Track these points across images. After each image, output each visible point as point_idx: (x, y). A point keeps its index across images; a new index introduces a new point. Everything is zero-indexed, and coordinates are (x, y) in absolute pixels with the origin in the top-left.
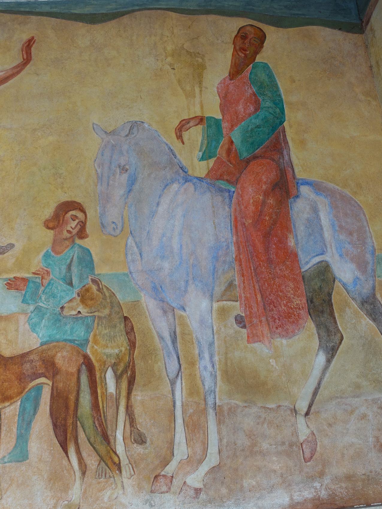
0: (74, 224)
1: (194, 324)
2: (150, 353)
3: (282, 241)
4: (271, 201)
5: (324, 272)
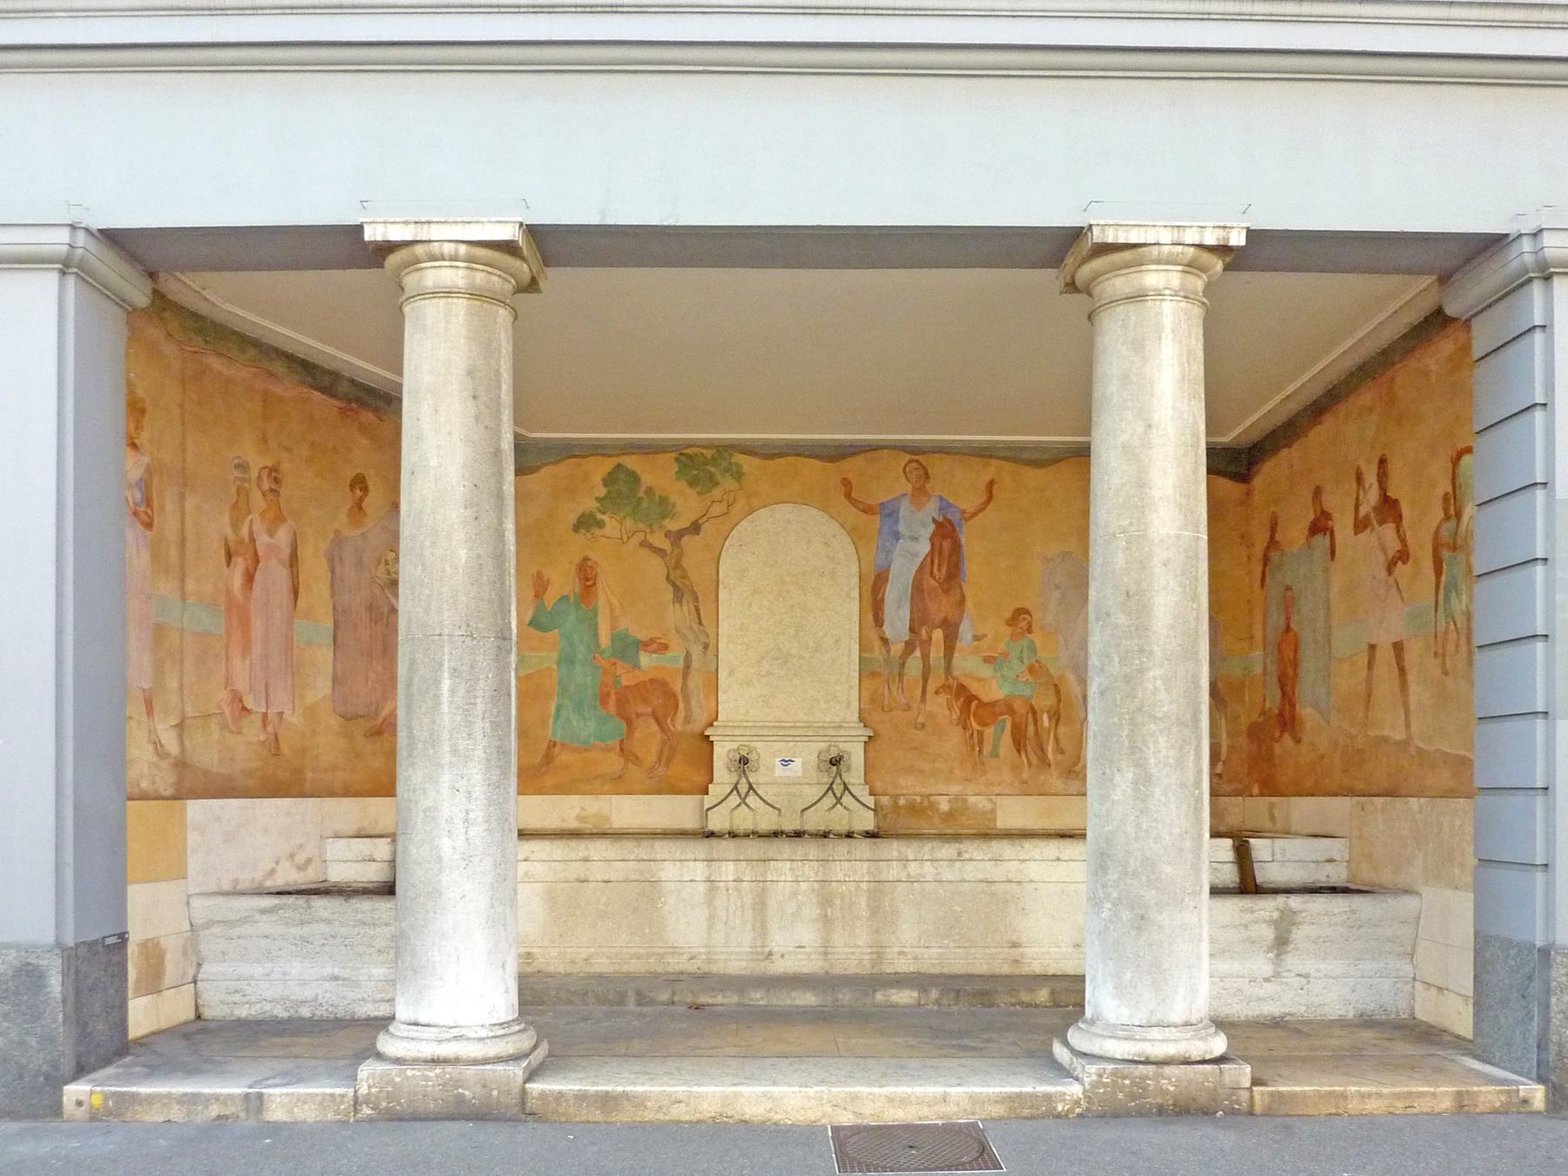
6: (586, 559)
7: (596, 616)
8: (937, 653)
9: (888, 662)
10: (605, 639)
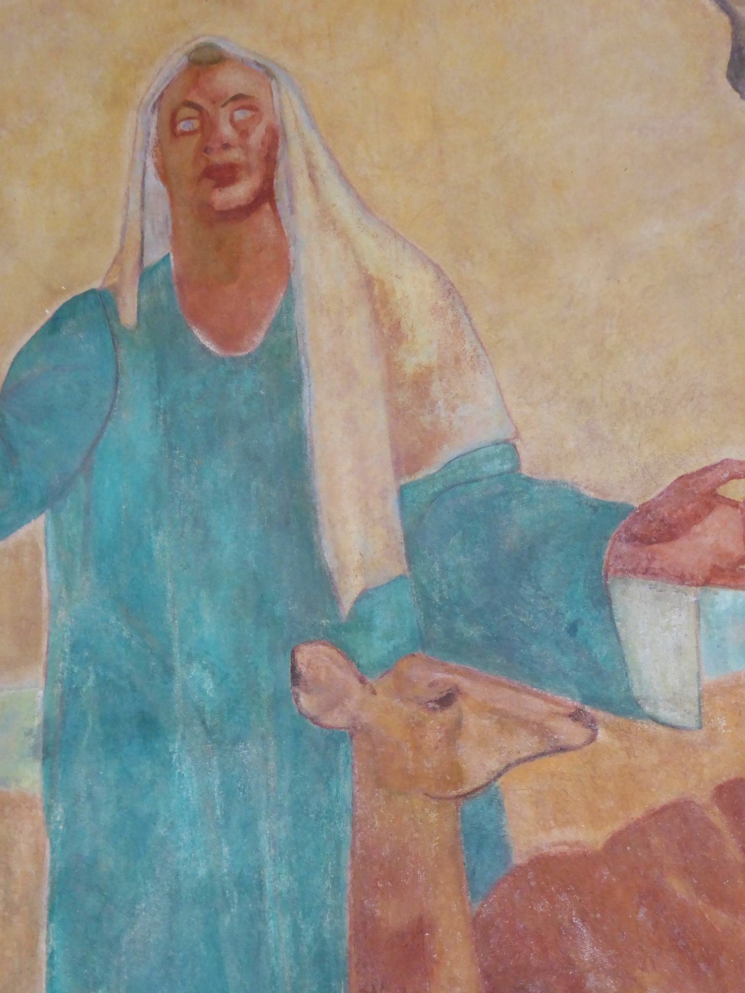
6: (205, 61)
7: (285, 379)
10: (359, 537)
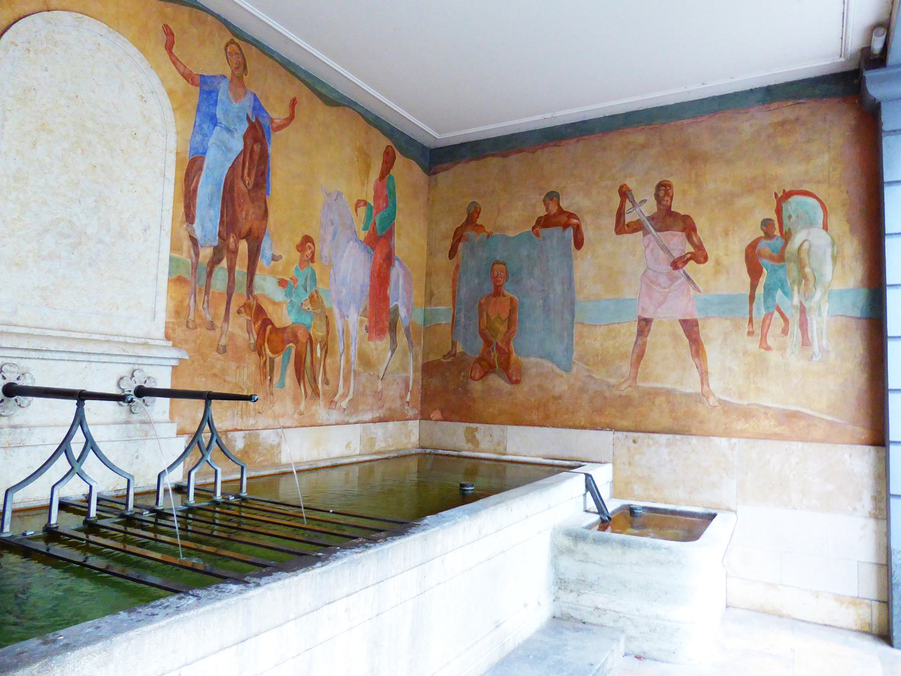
0: (309, 252)
1: (351, 327)
2: (334, 339)
3: (386, 290)
4: (385, 266)
5: (396, 309)
8: (241, 269)
9: (195, 266)
